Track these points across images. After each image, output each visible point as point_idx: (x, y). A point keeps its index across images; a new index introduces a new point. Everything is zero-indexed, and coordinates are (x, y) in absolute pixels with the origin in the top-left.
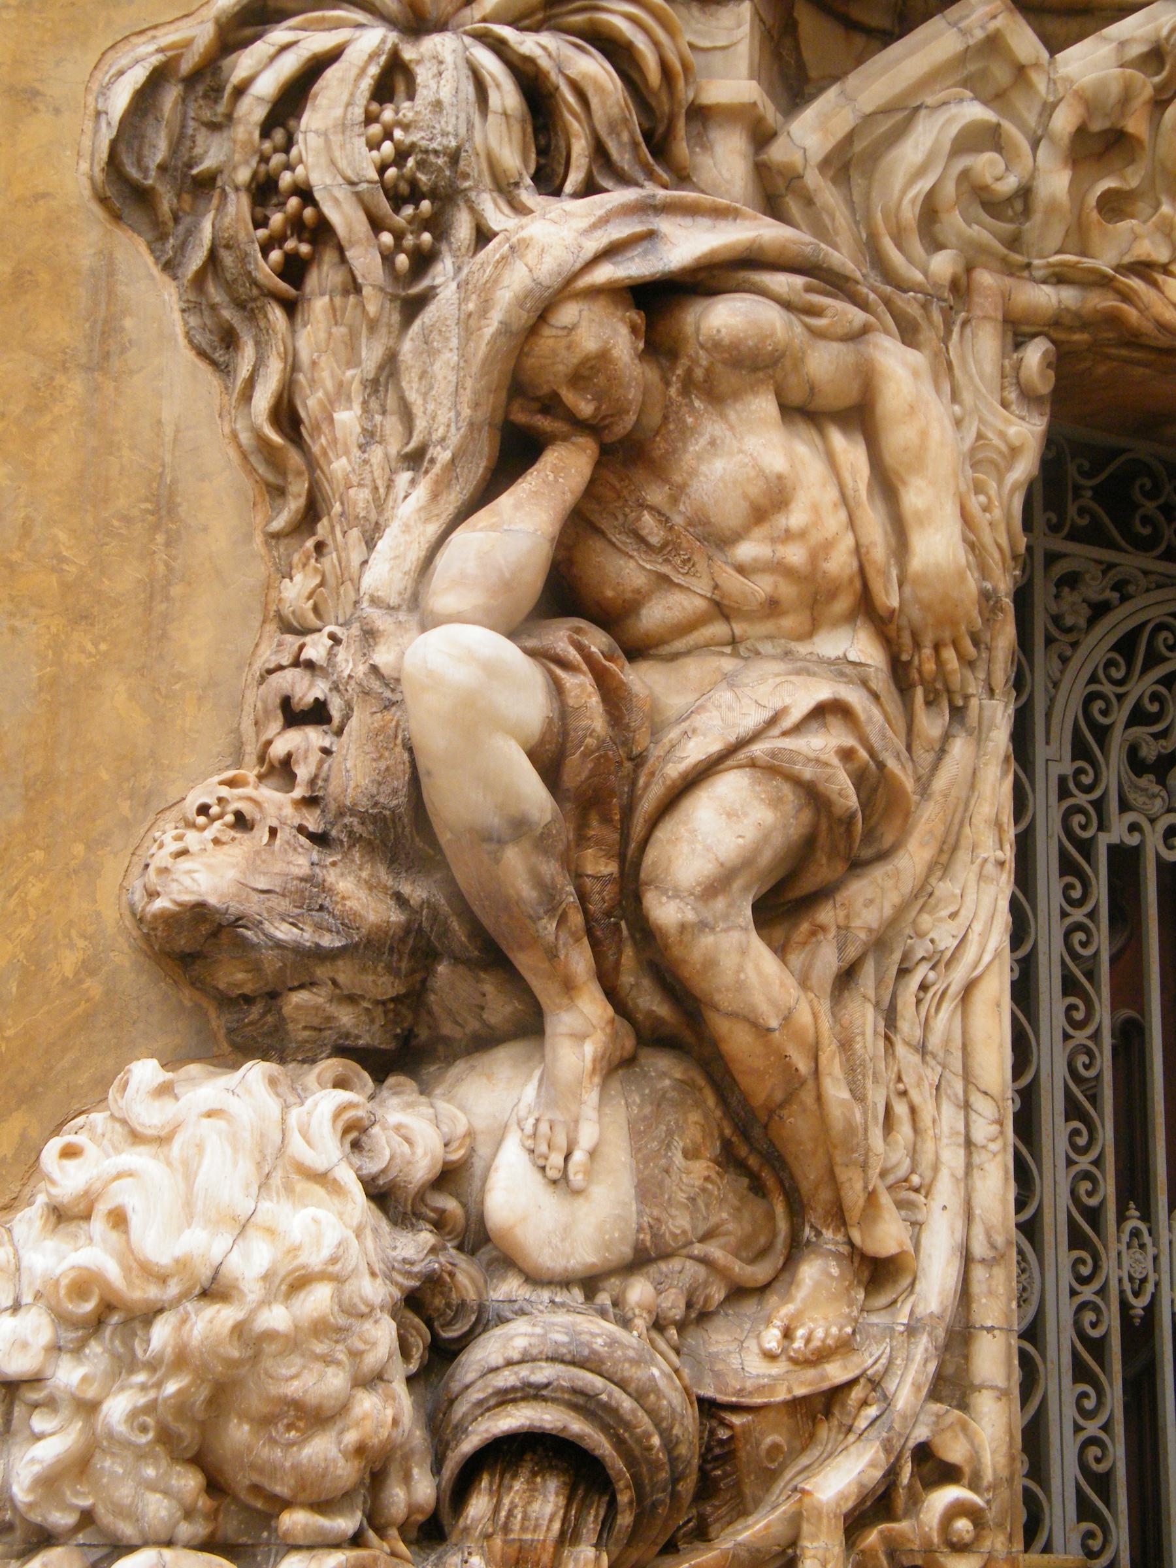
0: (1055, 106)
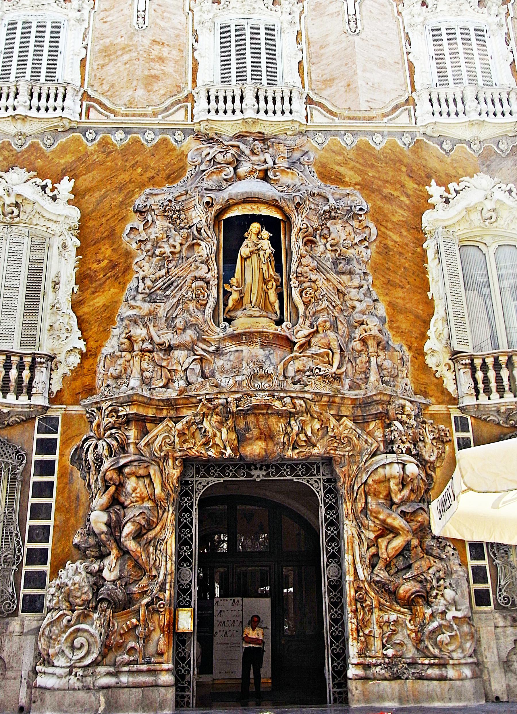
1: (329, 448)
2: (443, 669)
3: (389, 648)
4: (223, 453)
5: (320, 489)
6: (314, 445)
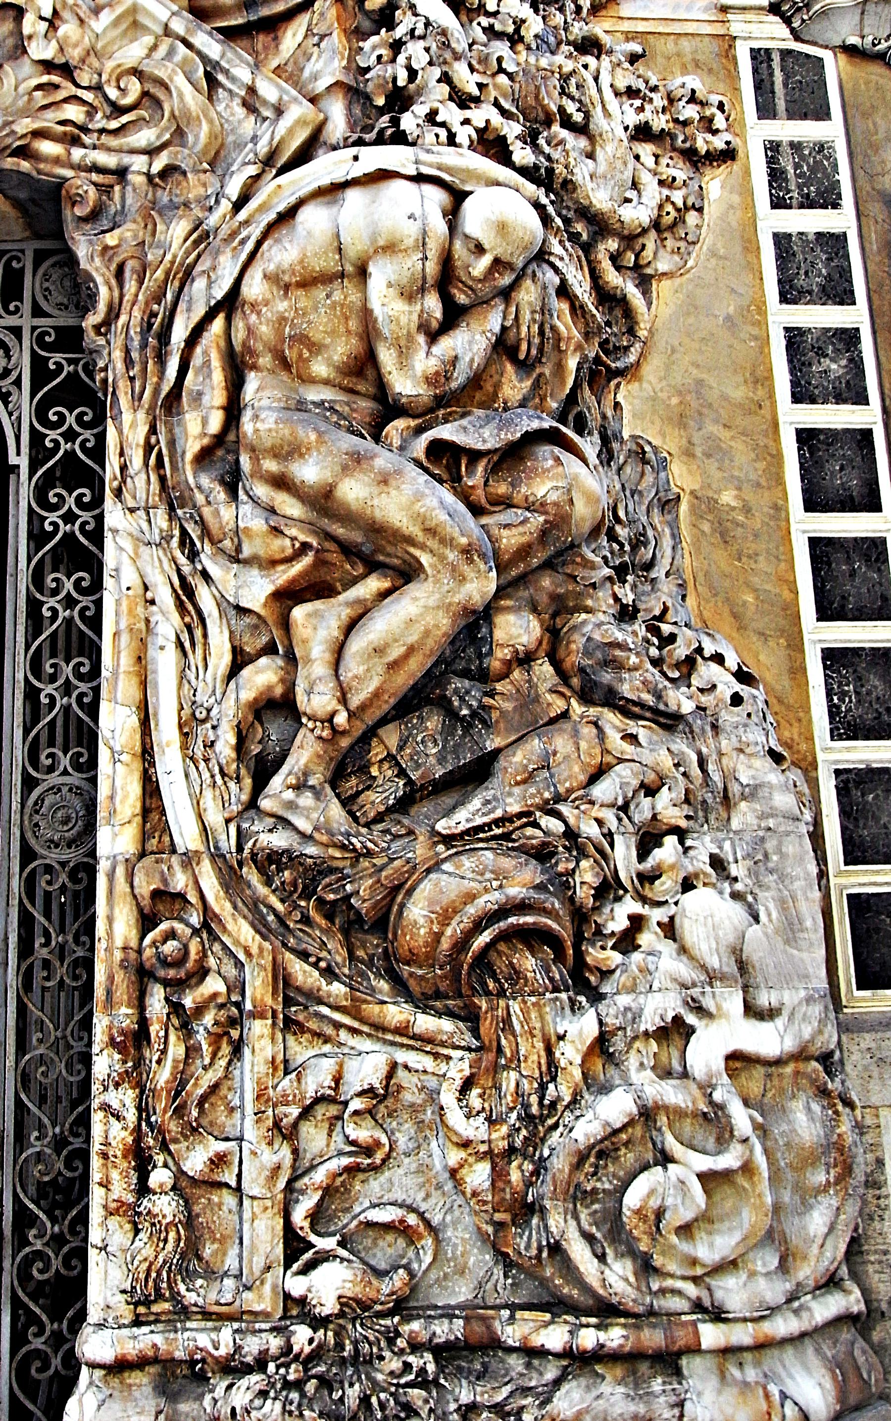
2: (657, 1385)
3: (324, 1257)
5: (18, 383)
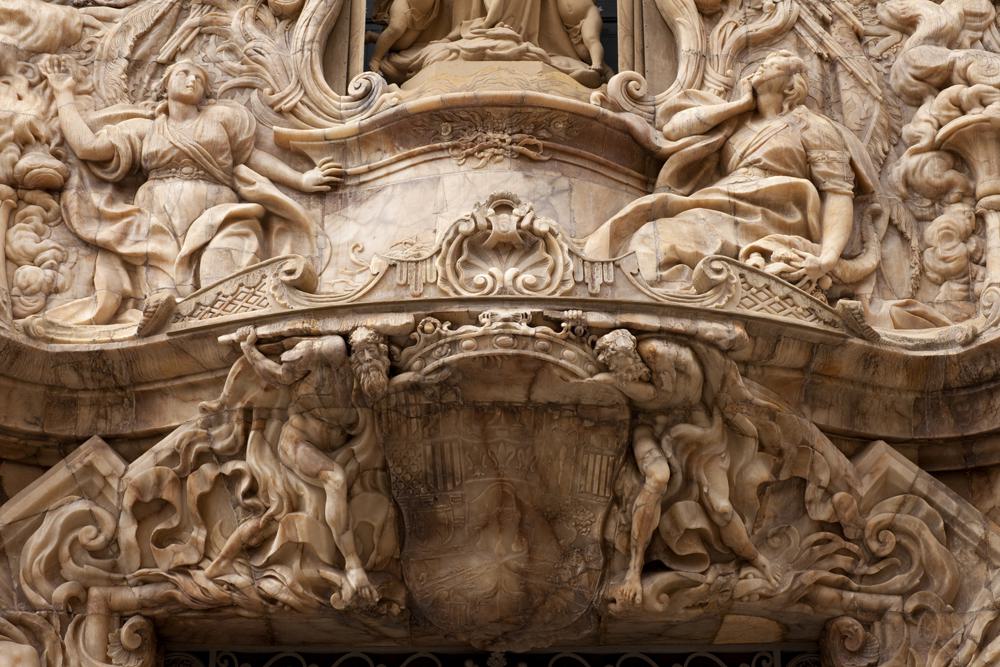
0: (123, 493)
1: (809, 576)
4: (325, 589)
6: (744, 561)
